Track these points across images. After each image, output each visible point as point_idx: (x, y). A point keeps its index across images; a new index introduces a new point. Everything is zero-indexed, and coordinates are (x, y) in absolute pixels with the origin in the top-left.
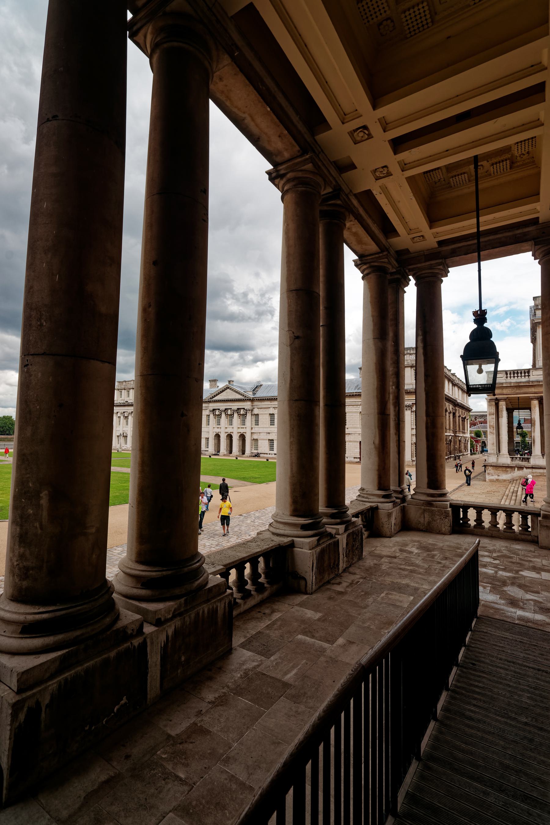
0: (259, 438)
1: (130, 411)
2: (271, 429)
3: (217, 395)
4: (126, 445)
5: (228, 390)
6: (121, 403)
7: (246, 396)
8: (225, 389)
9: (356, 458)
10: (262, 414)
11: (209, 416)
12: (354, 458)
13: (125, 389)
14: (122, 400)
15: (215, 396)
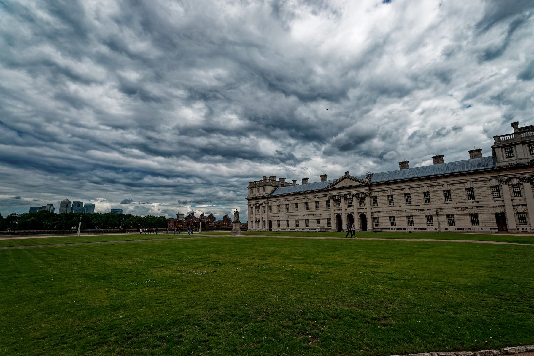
0: (379, 216)
1: (261, 203)
2: (391, 208)
3: (336, 184)
4: (252, 228)
5: (346, 179)
6: (253, 197)
7: (364, 183)
8: (343, 179)
9: (494, 229)
10: (379, 196)
11: (328, 202)
12: (491, 229)
13: (255, 187)
14: (254, 195)
15: (334, 185)
